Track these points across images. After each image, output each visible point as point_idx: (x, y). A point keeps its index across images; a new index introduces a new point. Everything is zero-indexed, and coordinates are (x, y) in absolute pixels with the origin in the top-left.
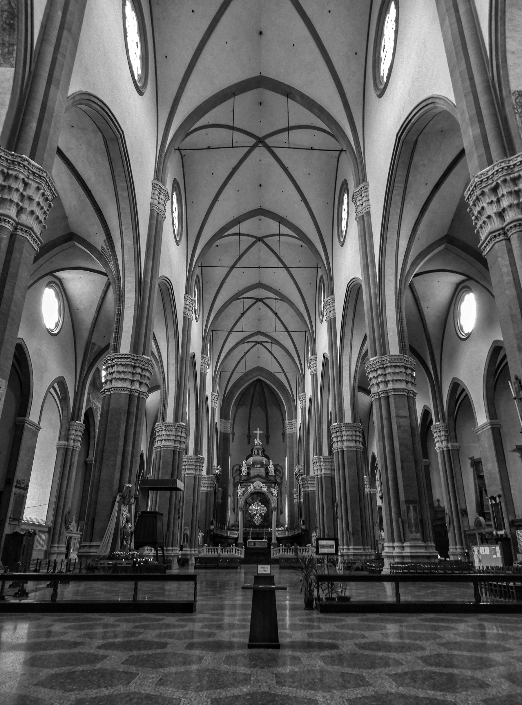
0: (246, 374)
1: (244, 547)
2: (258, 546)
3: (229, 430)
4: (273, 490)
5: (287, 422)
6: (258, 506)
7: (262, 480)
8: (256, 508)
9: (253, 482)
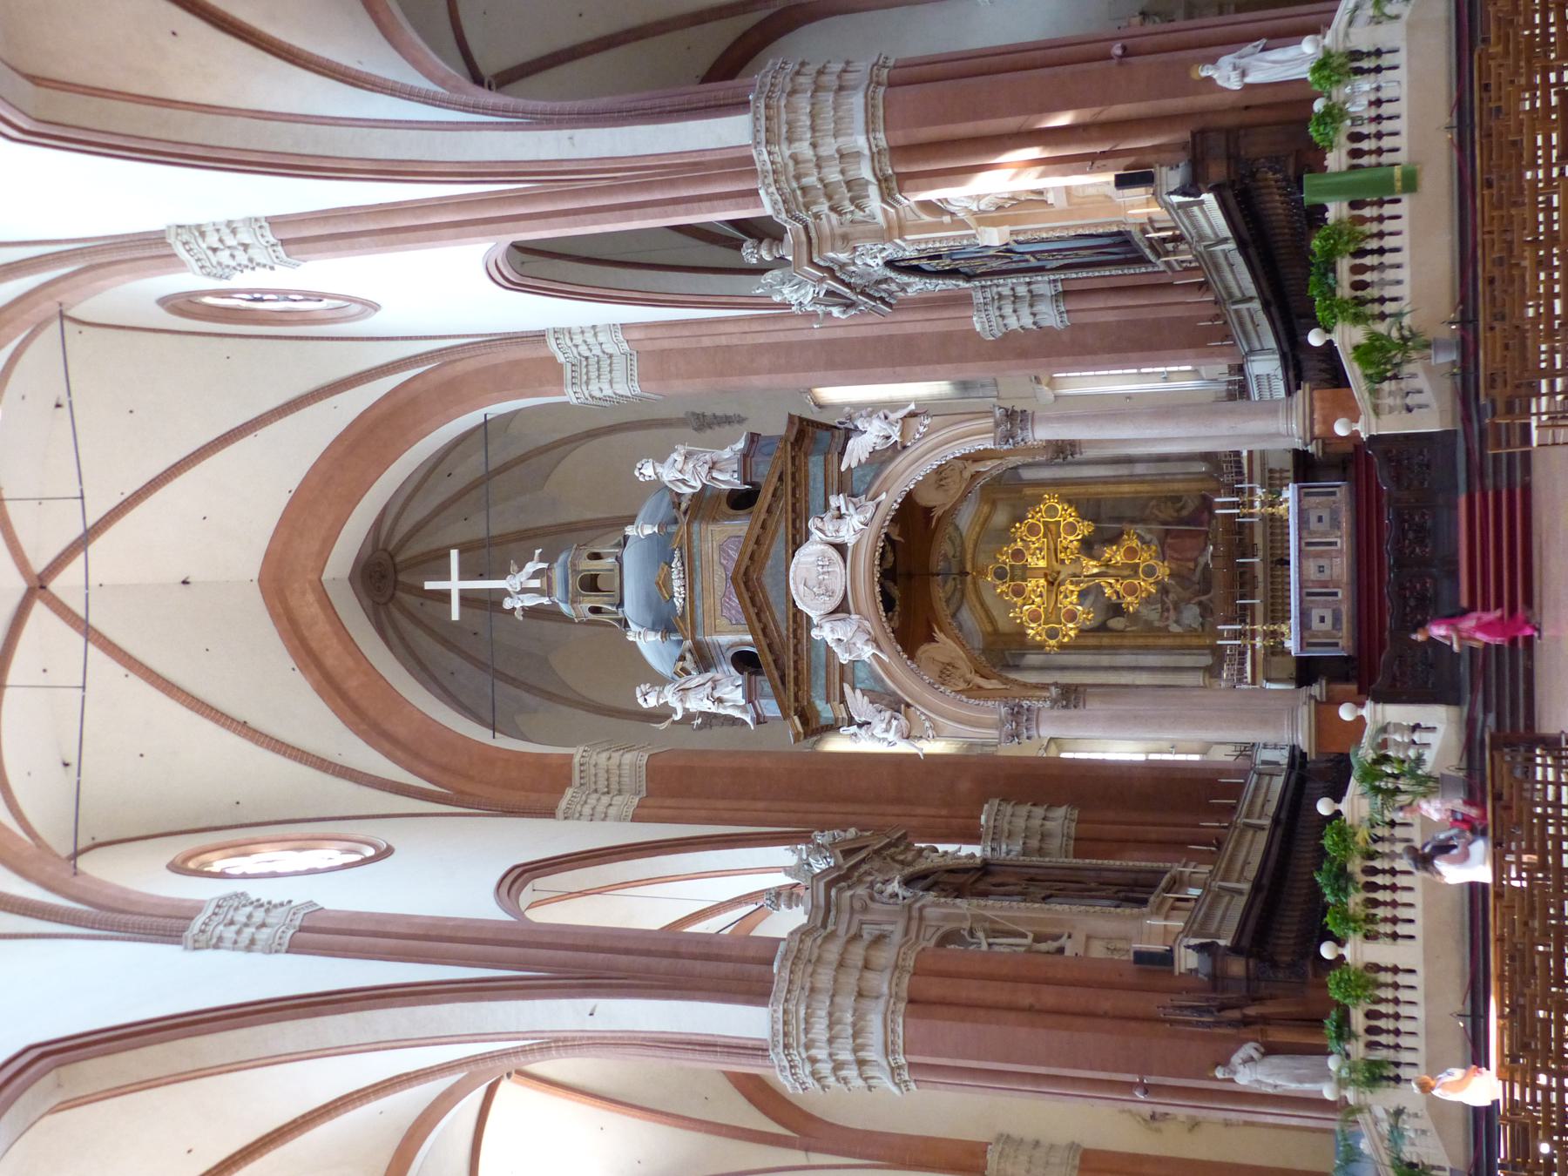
1: (1346, 713)
2: (1340, 567)
3: (633, 761)
4: (858, 450)
5: (570, 396)
6: (1026, 572)
7: (778, 547)
8: (1036, 584)
9: (800, 621)
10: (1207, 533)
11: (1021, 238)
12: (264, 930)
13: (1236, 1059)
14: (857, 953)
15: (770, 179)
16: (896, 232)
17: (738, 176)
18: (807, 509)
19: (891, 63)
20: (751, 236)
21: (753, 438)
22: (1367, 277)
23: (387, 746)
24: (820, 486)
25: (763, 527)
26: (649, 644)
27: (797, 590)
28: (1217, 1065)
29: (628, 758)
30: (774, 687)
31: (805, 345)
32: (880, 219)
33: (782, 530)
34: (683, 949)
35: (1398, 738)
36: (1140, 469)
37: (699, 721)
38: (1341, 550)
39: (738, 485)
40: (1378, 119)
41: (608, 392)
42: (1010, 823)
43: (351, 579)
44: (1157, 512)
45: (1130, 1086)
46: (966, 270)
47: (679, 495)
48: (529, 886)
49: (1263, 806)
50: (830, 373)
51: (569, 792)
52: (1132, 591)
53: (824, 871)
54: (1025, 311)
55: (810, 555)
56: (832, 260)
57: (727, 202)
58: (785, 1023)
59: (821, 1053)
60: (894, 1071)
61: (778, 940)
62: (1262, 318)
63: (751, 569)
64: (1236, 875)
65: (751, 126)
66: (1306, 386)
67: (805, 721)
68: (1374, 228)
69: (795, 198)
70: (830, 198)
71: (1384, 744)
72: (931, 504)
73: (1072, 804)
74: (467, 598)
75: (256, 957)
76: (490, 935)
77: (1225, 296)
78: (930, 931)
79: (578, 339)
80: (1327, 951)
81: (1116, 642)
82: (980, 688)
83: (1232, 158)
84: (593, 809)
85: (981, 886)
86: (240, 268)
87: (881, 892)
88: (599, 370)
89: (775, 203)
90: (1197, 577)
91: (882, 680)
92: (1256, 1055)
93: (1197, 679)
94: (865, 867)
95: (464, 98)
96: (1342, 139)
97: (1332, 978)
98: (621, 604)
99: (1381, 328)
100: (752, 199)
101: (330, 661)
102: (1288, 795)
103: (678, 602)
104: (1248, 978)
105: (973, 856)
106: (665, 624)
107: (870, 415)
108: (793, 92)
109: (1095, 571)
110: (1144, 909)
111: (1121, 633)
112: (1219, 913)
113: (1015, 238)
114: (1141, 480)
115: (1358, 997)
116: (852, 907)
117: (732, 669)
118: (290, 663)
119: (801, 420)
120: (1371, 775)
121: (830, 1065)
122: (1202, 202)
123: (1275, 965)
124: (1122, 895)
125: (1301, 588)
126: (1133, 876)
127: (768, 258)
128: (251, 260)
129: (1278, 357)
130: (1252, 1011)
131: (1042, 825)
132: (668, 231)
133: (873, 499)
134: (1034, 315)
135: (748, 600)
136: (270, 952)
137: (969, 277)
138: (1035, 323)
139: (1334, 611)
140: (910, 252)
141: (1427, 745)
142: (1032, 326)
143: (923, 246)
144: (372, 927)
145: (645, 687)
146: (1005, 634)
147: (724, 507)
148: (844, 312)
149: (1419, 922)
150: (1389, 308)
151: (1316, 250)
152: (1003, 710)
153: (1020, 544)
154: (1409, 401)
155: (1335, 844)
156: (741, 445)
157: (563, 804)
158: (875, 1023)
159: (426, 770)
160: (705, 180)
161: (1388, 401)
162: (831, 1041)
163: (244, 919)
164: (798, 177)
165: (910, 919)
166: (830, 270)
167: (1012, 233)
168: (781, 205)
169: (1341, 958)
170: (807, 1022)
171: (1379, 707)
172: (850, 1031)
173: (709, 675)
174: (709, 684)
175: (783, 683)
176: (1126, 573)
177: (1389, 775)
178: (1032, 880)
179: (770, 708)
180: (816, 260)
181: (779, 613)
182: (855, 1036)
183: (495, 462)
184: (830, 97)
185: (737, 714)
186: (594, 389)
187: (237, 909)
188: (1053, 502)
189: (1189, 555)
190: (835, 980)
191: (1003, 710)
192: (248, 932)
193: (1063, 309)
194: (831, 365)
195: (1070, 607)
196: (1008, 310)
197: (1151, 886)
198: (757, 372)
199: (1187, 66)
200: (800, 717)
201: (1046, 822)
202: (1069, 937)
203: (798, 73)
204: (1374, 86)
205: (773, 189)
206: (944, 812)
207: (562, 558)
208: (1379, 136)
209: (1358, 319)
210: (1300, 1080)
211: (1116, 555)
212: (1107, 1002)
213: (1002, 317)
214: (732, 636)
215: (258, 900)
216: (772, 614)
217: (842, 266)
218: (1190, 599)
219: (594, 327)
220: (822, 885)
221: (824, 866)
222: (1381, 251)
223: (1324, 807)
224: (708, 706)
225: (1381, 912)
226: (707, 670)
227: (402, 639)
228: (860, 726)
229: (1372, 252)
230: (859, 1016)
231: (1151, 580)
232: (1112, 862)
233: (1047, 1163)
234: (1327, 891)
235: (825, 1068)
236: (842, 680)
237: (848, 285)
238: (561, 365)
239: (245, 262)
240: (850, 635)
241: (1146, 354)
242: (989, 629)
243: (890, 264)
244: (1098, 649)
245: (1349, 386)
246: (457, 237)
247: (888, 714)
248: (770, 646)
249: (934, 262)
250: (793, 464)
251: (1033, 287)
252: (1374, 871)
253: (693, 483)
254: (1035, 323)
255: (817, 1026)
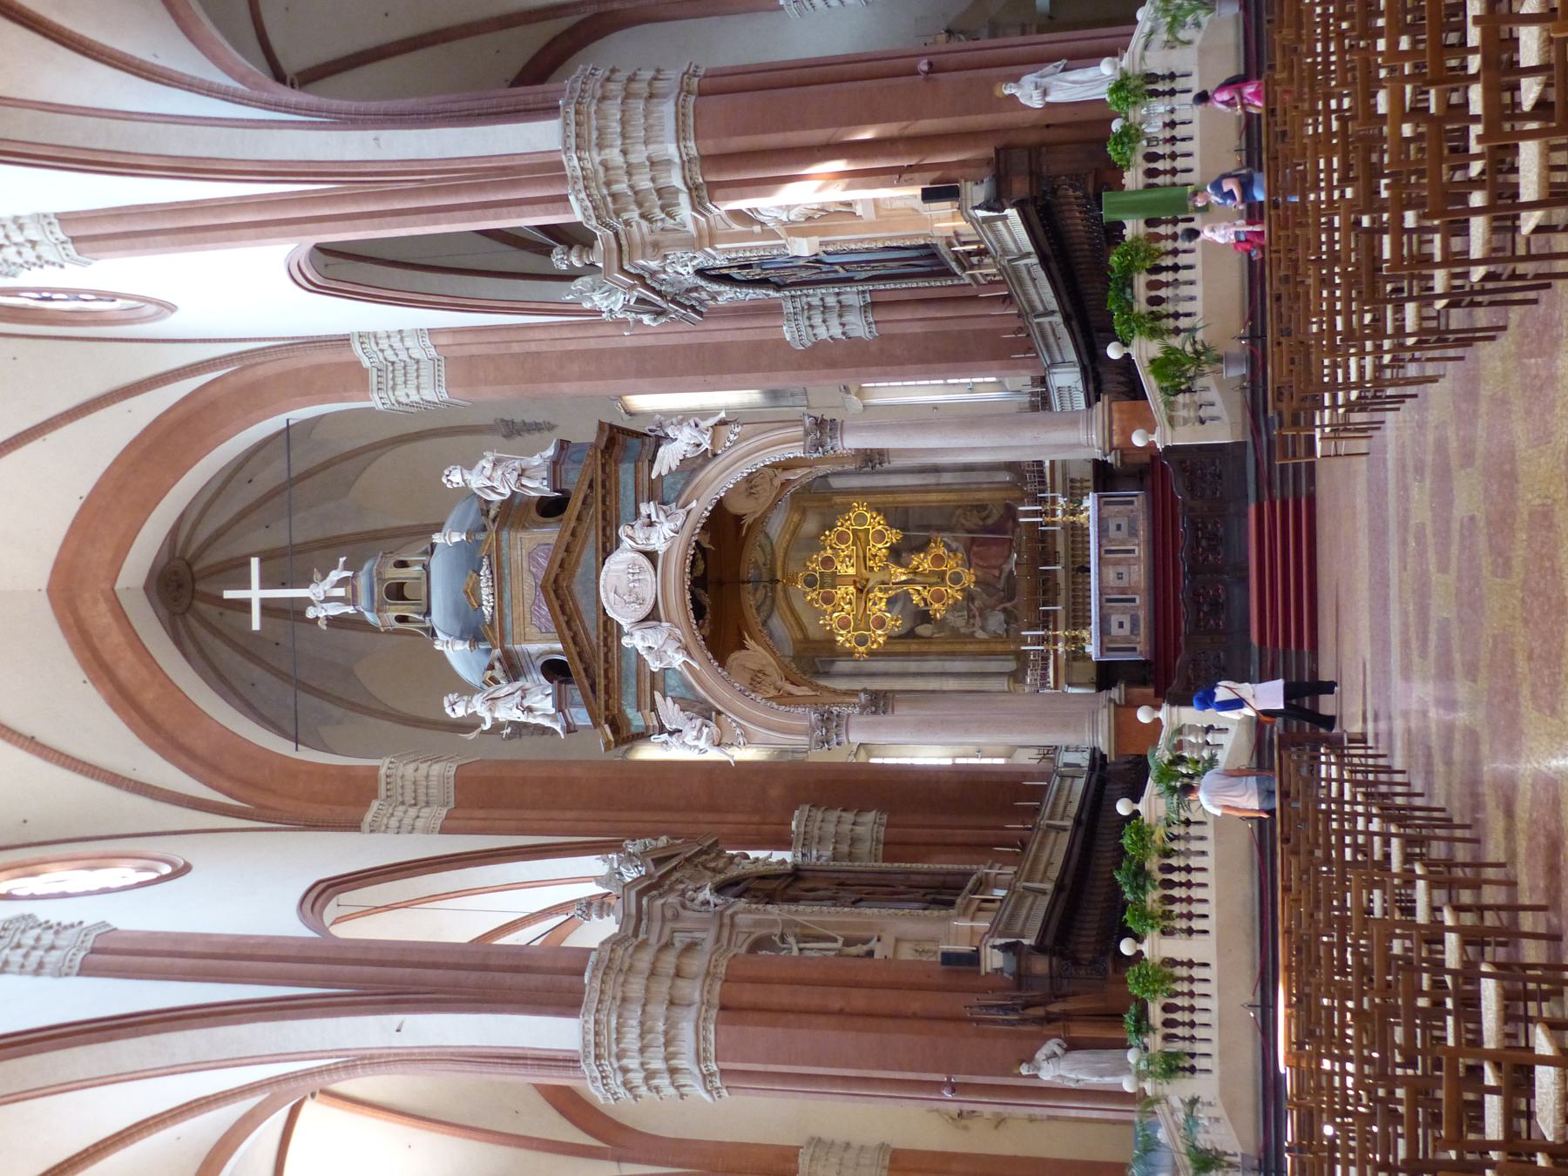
0: (97, 665)
1: (1144, 716)
2: (1137, 574)
3: (441, 772)
4: (668, 458)
5: (375, 401)
6: (835, 580)
7: (588, 555)
8: (845, 591)
9: (610, 629)
10: (1011, 540)
11: (830, 249)
12: (54, 953)
13: (1040, 1056)
14: (669, 961)
15: (580, 185)
16: (706, 241)
17: (549, 181)
18: (618, 517)
19: (702, 72)
20: (561, 242)
21: (563, 445)
22: (1163, 293)
23: (185, 760)
24: (631, 494)
25: (573, 534)
26: (457, 653)
27: (607, 598)
28: (1021, 1062)
29: (436, 769)
30: (584, 696)
31: (616, 352)
32: (691, 227)
33: (592, 538)
34: (492, 961)
35: (1193, 740)
36: (947, 478)
37: (509, 730)
38: (1139, 557)
39: (547, 492)
40: (1173, 140)
41: (415, 397)
42: (820, 828)
43: (146, 588)
44: (964, 521)
45: (938, 1086)
46: (776, 279)
47: (488, 502)
48: (333, 903)
49: (1065, 808)
50: (640, 381)
51: (375, 805)
52: (939, 598)
53: (635, 880)
54: (834, 322)
55: (621, 562)
56: (643, 267)
57: (536, 207)
58: (596, 1034)
59: (633, 1063)
60: (706, 1078)
61: (590, 950)
62: (1063, 331)
63: (561, 578)
64: (1039, 876)
65: (561, 131)
66: (1105, 398)
67: (616, 730)
68: (1168, 245)
69: (605, 204)
70: (640, 205)
71: (1180, 746)
72: (743, 512)
73: (881, 810)
74: (266, 606)
75: (44, 981)
76: (292, 953)
77: (1028, 309)
78: (742, 937)
79: (384, 344)
80: (1127, 947)
81: (925, 648)
82: (790, 694)
83: (1035, 175)
84: (400, 821)
85: (791, 892)
86: (28, 265)
87: (693, 900)
88: (405, 375)
89: (585, 209)
90: (1001, 584)
91: (693, 688)
92: (1059, 1051)
93: (1002, 684)
94: (677, 875)
95: (265, 96)
96: (1138, 159)
97: (1131, 974)
98: (428, 613)
99: (1176, 342)
100: (561, 204)
101: (123, 673)
102: (1089, 797)
103: (487, 610)
104: (1051, 977)
105: (783, 862)
106: (474, 633)
107: (680, 423)
108: (603, 98)
109: (904, 578)
110: (952, 912)
111: (928, 639)
112: (1024, 912)
113: (824, 248)
114: (948, 489)
115: (1155, 992)
116: (663, 915)
117: (542, 678)
118: (80, 675)
119: (611, 427)
120: (1166, 775)
121: (642, 1075)
122: (1006, 217)
123: (1076, 962)
124: (929, 897)
125: (1101, 594)
126: (941, 878)
127: (578, 264)
128: (39, 257)
129: (1078, 369)
130: (1056, 1008)
131: (852, 830)
132: (478, 236)
133: (683, 507)
134: (843, 325)
135: (557, 608)
136: (60, 976)
137: (778, 287)
138: (844, 333)
139: (1132, 616)
140: (721, 261)
141: (1220, 746)
142: (840, 336)
143: (733, 255)
144: (166, 947)
145: (453, 697)
146: (816, 641)
147: (534, 514)
148: (655, 319)
149: (1213, 917)
150: (1183, 323)
151: (1115, 265)
152: (814, 717)
153: (829, 551)
154: (1203, 413)
155: (1134, 843)
156: (550, 452)
157: (368, 817)
158: (687, 1030)
159: (226, 785)
160: (513, 184)
161: (1182, 413)
162: (642, 1051)
163: (31, 942)
164: (608, 184)
165: (721, 926)
166: (640, 277)
167: (821, 244)
168: (591, 211)
169: (1140, 953)
170: (618, 1032)
171: (1175, 709)
172: (662, 1040)
173: (518, 684)
174: (519, 692)
175: (594, 691)
176: (934, 580)
177: (1184, 776)
178: (842, 884)
179: (581, 717)
180: (626, 267)
181: (590, 620)
182: (667, 1044)
183: (299, 467)
184: (641, 105)
185: (547, 723)
186: (401, 394)
187: (24, 931)
188: (862, 510)
189: (993, 562)
190: (647, 989)
191: (814, 717)
192: (36, 956)
193: (871, 320)
194: (641, 373)
195: (879, 614)
196: (817, 320)
197: (958, 888)
198: (563, 379)
199: (991, 84)
200: (610, 727)
201: (859, 829)
202: (879, 940)
203: (608, 80)
204: (1168, 108)
205: (583, 195)
206: (756, 819)
207: (367, 566)
208: (1173, 156)
209: (1154, 333)
210: (1101, 1074)
211: (923, 562)
212: (917, 1002)
213: (812, 326)
214: (542, 645)
215: (47, 922)
216: (582, 622)
217: (653, 274)
218: (995, 606)
219: (400, 332)
220: (633, 894)
221: (635, 875)
222: (1176, 268)
223: (1123, 808)
224: (518, 716)
225: (1177, 908)
226: (516, 680)
227: (201, 651)
228: (671, 733)
229: (1167, 269)
230: (671, 1024)
231: (958, 587)
232: (920, 865)
233: (858, 1165)
234: (1126, 889)
235: (637, 1078)
236: (653, 688)
237: (659, 293)
238: (367, 370)
239: (34, 260)
240: (661, 642)
241: (950, 365)
242: (800, 636)
243: (701, 272)
244: (907, 655)
245: (1146, 398)
246: (258, 238)
247: (698, 722)
248: (580, 654)
249: (745, 272)
250: (604, 471)
251: (842, 297)
252: (1170, 869)
253: (501, 490)
254: (844, 333)
255: (629, 1036)
